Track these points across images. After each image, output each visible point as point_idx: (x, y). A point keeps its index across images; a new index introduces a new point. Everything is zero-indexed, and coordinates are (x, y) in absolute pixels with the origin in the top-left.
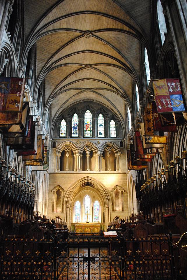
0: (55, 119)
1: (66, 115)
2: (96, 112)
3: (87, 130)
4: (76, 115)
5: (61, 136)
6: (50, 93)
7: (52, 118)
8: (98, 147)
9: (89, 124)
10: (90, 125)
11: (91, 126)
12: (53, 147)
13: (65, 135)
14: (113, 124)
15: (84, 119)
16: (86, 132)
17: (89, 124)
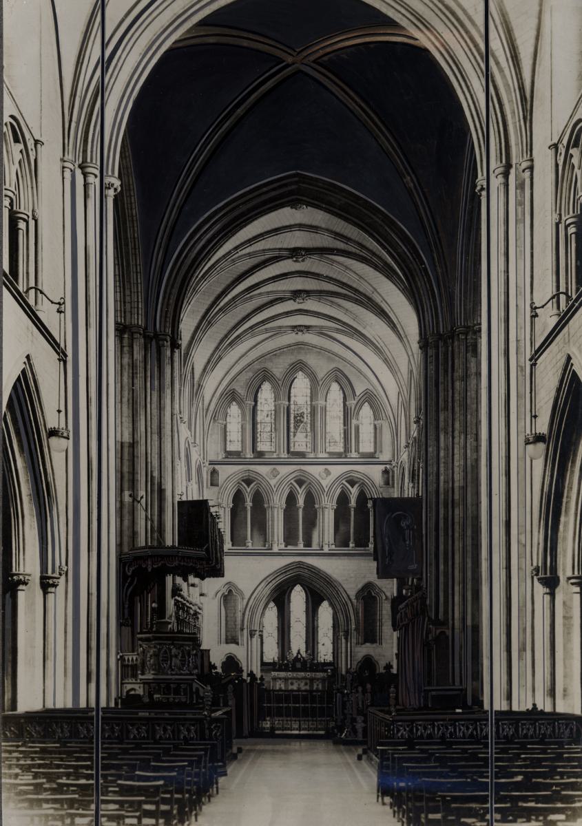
0: (212, 408)
1: (241, 391)
2: (321, 383)
3: (297, 430)
4: (266, 387)
5: (230, 448)
6: (205, 361)
7: (206, 402)
8: (326, 484)
9: (303, 413)
10: (305, 416)
11: (307, 419)
12: (212, 485)
13: (240, 446)
14: (366, 411)
15: (289, 400)
16: (294, 436)
17: (303, 413)
